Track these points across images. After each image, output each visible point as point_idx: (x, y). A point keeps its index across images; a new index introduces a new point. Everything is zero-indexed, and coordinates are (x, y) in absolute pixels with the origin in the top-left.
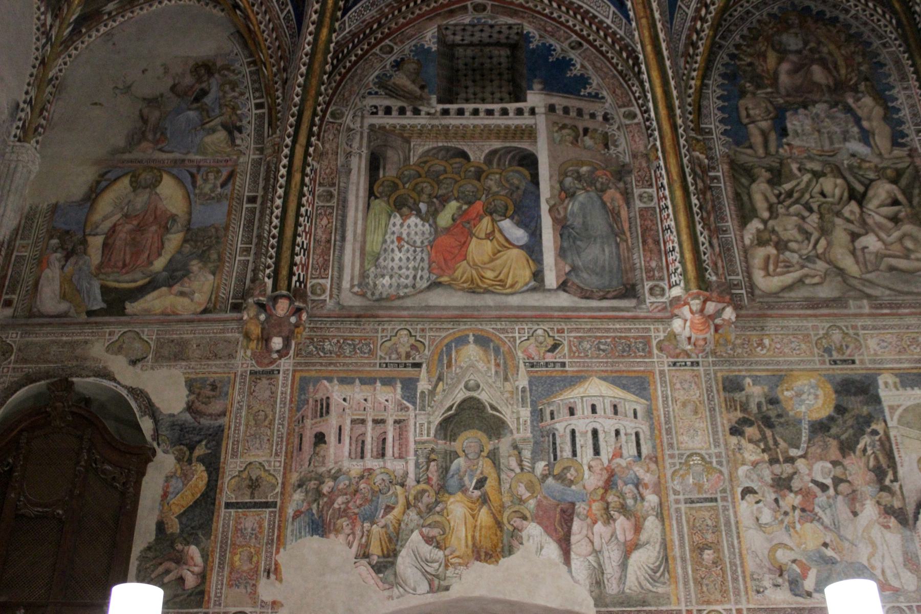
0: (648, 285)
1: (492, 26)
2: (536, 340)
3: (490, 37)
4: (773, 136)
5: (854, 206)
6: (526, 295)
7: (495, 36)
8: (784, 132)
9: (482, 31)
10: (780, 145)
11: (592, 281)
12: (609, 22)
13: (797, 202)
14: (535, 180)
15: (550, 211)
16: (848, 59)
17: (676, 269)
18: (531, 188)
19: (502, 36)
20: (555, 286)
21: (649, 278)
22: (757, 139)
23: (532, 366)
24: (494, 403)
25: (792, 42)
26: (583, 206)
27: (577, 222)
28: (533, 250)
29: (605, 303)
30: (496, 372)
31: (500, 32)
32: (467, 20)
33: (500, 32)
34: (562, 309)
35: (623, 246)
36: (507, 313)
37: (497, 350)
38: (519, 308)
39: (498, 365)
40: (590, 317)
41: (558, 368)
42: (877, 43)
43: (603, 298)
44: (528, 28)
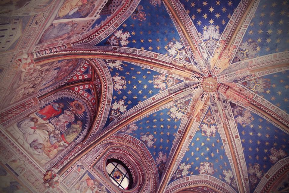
0: (39, 47)
1: (117, 6)
2: (41, 18)
3: (114, 3)
4: (56, 68)
5: (32, 85)
6: (56, 15)
7: (114, 4)
8: (55, 69)
9: (118, 3)
10: (53, 69)
11: (48, 33)
12: (101, 35)
13: (39, 75)
14: (82, 17)
15: (72, 21)
16: (61, 78)
17: (40, 55)
18: (81, 16)
19: (112, 6)
20: (53, 22)
21: (41, 47)
22: (57, 65)
23: (34, 17)
24: (29, 4)
25: (71, 68)
26: (68, 29)
27: (65, 28)
28: (67, 17)
29: (41, 35)
30: (39, 5)
31: (114, 6)
32: (123, 2)
33: (114, 6)
34: (46, 25)
35: (52, 39)
36: (54, 10)
37: (45, 6)
38: (54, 13)
39: (41, 6)
40: (39, 32)
41: (30, 24)
42: (61, 82)
43: (42, 35)
44: (112, 15)
